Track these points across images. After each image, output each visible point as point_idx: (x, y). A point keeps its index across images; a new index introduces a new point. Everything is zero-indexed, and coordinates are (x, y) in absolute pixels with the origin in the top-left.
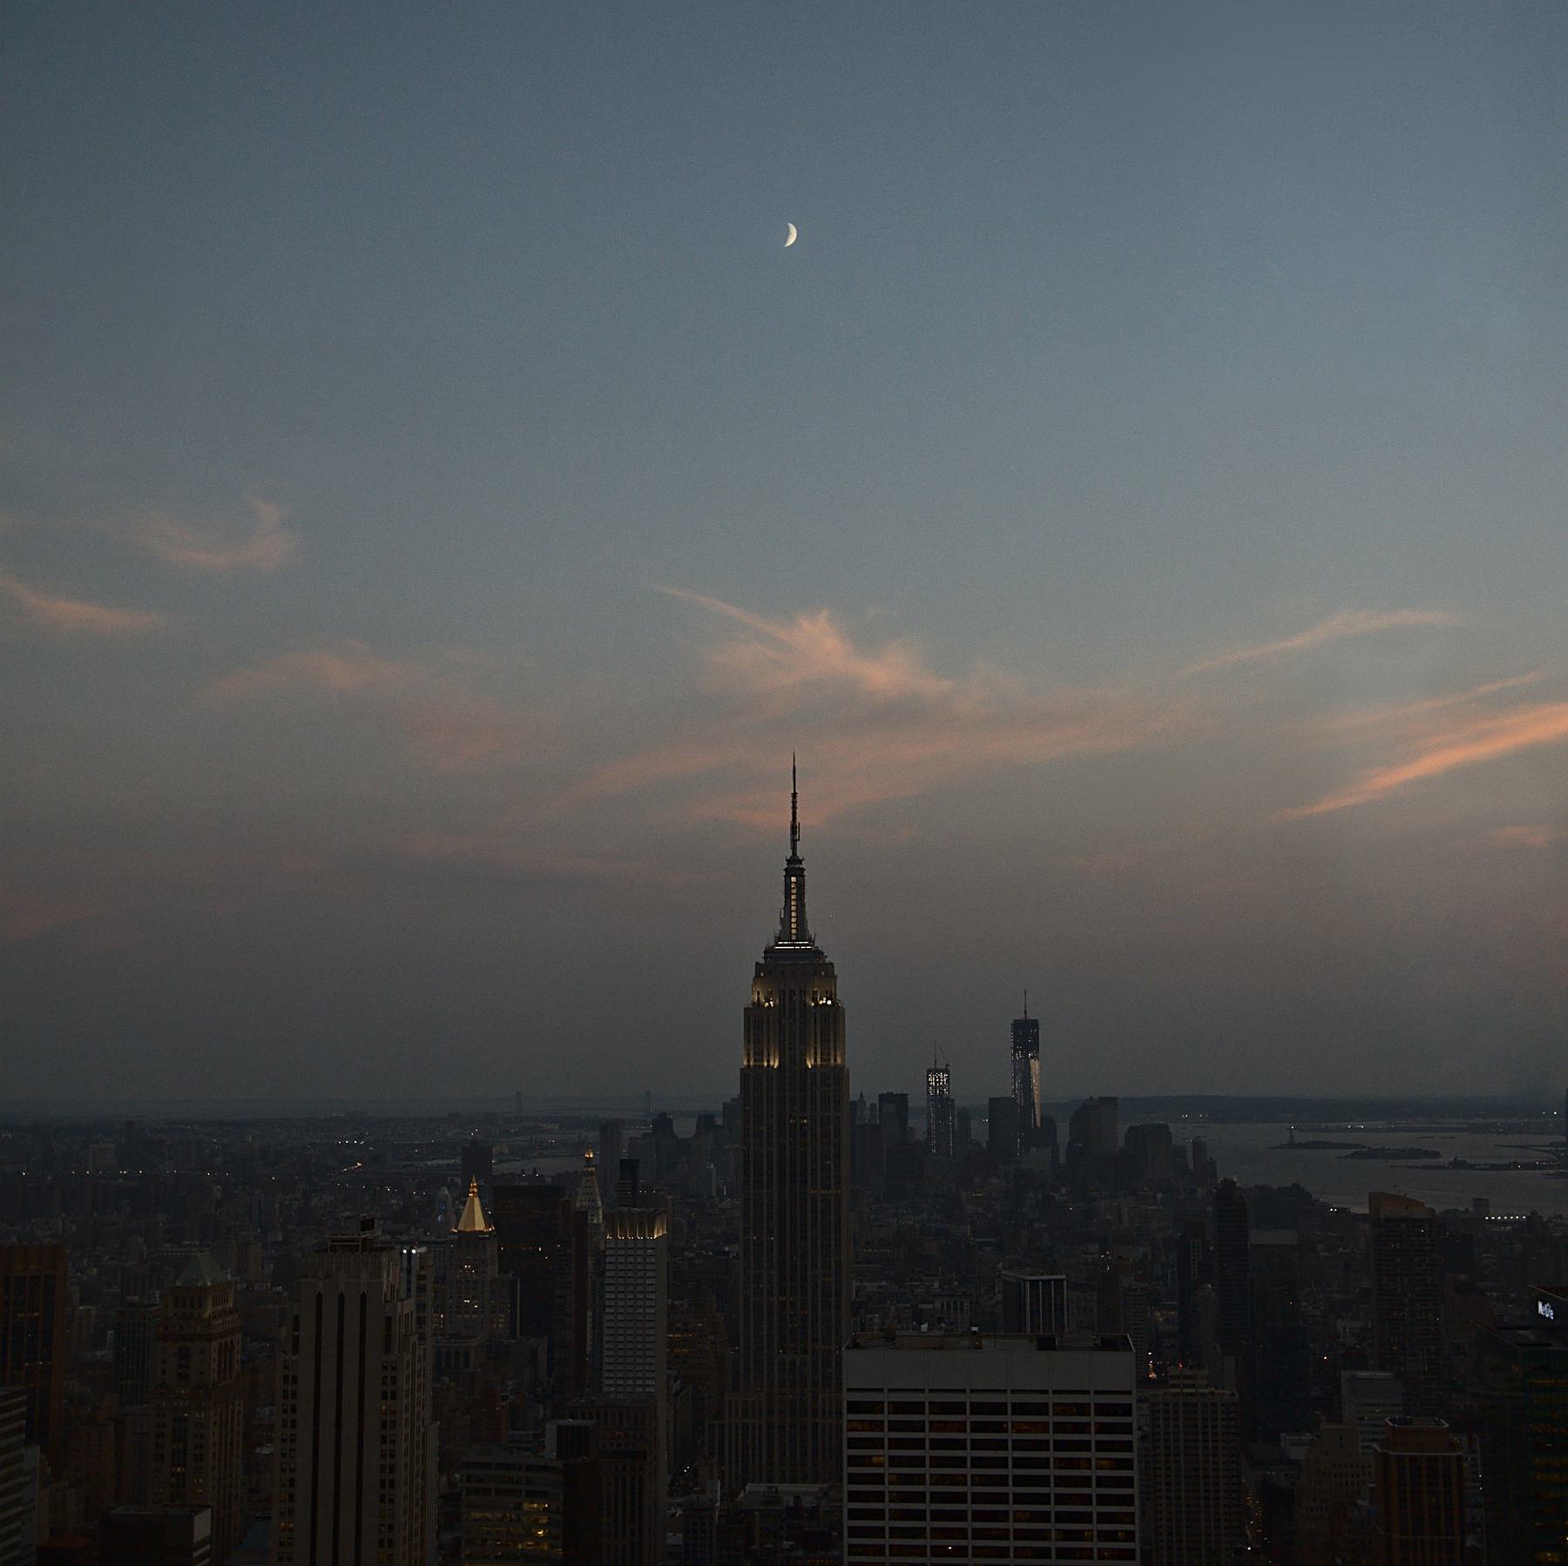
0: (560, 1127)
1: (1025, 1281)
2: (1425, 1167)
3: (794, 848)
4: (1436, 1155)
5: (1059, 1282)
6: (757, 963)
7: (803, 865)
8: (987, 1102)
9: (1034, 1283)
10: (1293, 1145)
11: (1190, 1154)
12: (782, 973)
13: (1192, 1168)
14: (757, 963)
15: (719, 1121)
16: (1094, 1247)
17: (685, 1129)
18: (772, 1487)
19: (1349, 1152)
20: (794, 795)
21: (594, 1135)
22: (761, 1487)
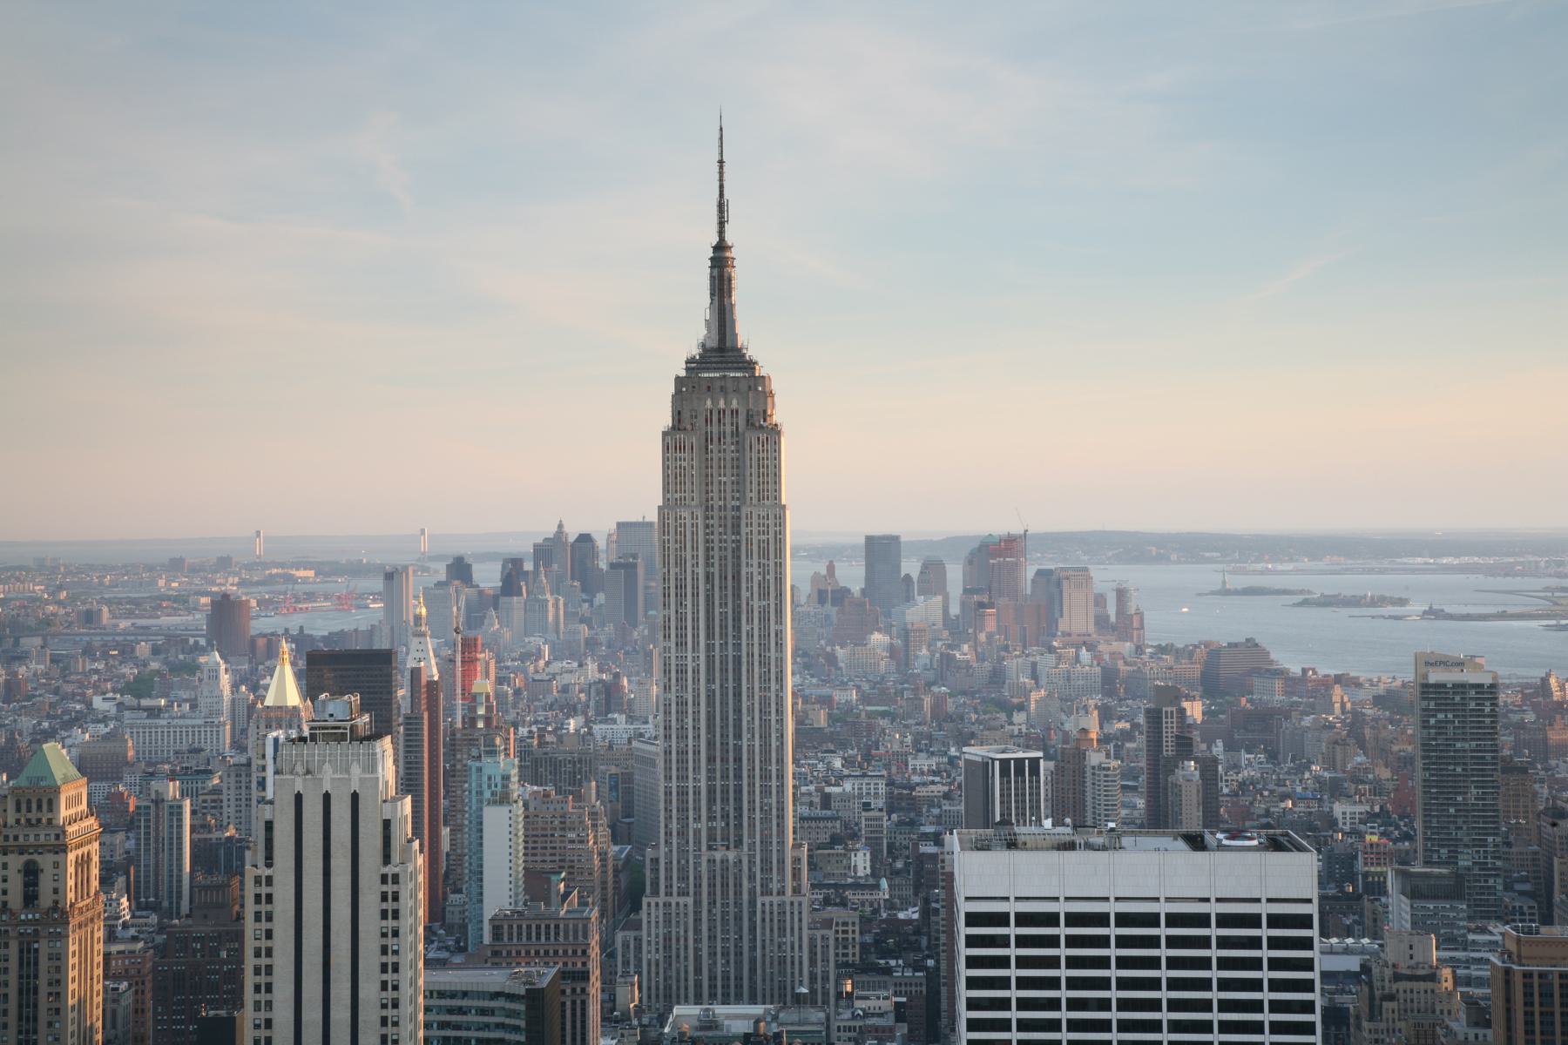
0: (317, 575)
1: (993, 760)
2: (1391, 617)
3: (721, 232)
5: (1035, 763)
6: (678, 379)
7: (733, 253)
8: (863, 541)
9: (1005, 764)
10: (1226, 592)
12: (709, 387)
13: (1113, 619)
14: (678, 379)
16: (1019, 718)
18: (708, 1010)
19: (1300, 598)
20: (721, 162)
21: (378, 584)
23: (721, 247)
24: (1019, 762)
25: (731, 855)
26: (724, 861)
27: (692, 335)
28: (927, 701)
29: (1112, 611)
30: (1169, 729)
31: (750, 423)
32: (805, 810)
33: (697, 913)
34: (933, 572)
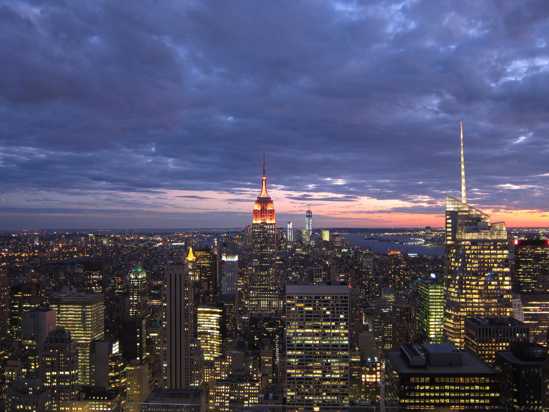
19: (379, 240)
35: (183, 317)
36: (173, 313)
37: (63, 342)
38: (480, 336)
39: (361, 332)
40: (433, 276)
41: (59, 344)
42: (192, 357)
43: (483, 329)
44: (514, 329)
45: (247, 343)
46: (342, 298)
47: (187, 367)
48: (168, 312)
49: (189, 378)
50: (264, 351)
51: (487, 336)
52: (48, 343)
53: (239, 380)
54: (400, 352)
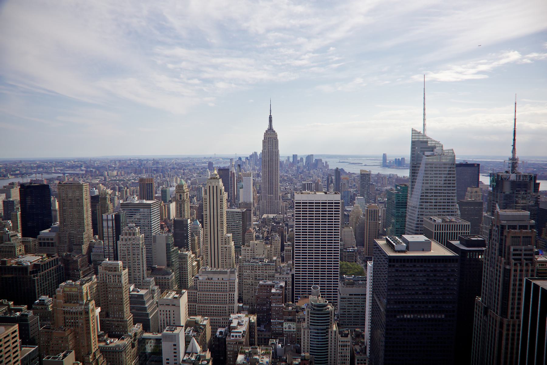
4: (362, 164)
5: (311, 184)
10: (339, 162)
11: (325, 163)
15: (249, 158)
16: (312, 178)
17: (244, 160)
21: (229, 160)
22: (266, 215)
23: (270, 116)
24: (309, 184)
25: (271, 195)
26: (270, 196)
27: (266, 127)
28: (300, 176)
29: (325, 164)
30: (330, 180)
31: (274, 139)
32: (282, 190)
33: (267, 203)
34: (302, 159)
35: (219, 217)
36: (212, 214)
37: (134, 235)
38: (435, 230)
39: (343, 228)
40: (399, 188)
41: (131, 236)
42: (226, 246)
43: (438, 225)
44: (460, 225)
45: (261, 236)
46: (335, 203)
47: (222, 253)
48: (208, 214)
49: (224, 260)
50: (275, 242)
51: (440, 230)
52: (124, 236)
53: (260, 261)
54: (385, 241)
